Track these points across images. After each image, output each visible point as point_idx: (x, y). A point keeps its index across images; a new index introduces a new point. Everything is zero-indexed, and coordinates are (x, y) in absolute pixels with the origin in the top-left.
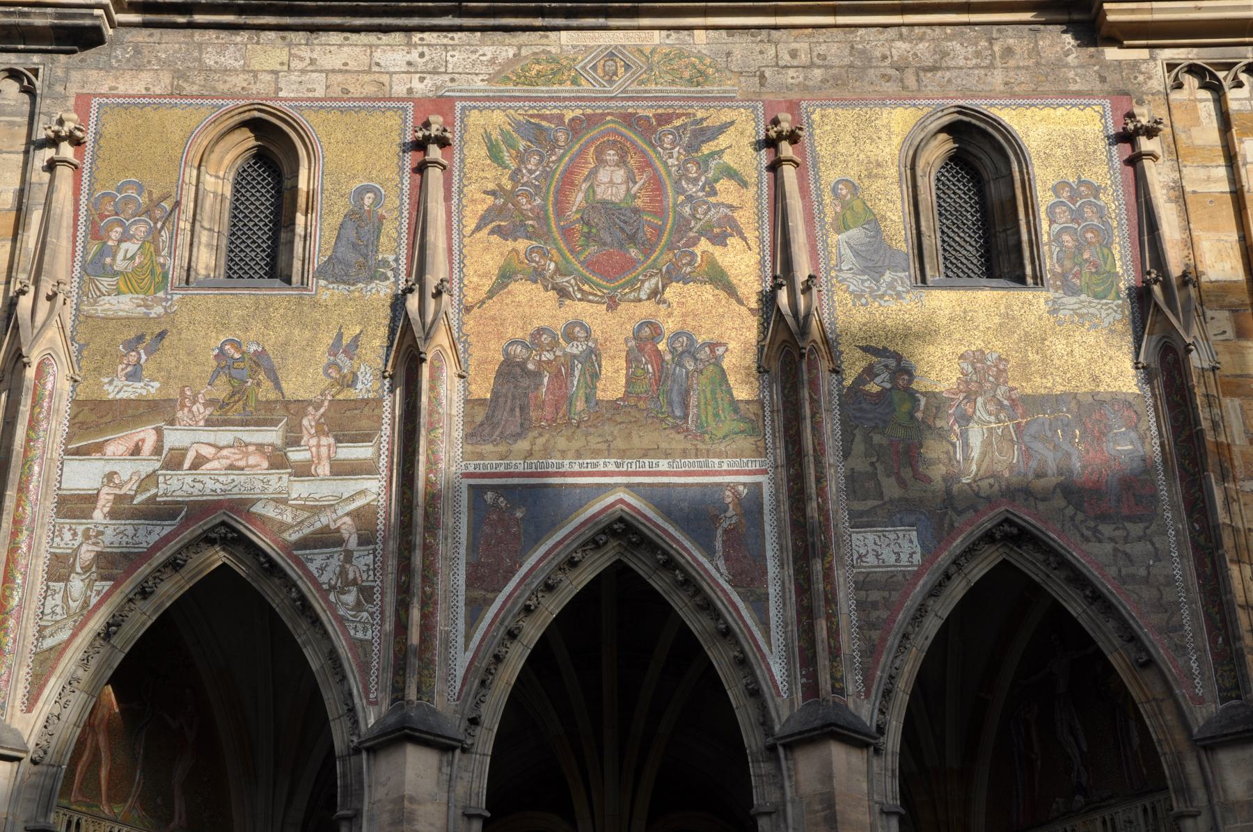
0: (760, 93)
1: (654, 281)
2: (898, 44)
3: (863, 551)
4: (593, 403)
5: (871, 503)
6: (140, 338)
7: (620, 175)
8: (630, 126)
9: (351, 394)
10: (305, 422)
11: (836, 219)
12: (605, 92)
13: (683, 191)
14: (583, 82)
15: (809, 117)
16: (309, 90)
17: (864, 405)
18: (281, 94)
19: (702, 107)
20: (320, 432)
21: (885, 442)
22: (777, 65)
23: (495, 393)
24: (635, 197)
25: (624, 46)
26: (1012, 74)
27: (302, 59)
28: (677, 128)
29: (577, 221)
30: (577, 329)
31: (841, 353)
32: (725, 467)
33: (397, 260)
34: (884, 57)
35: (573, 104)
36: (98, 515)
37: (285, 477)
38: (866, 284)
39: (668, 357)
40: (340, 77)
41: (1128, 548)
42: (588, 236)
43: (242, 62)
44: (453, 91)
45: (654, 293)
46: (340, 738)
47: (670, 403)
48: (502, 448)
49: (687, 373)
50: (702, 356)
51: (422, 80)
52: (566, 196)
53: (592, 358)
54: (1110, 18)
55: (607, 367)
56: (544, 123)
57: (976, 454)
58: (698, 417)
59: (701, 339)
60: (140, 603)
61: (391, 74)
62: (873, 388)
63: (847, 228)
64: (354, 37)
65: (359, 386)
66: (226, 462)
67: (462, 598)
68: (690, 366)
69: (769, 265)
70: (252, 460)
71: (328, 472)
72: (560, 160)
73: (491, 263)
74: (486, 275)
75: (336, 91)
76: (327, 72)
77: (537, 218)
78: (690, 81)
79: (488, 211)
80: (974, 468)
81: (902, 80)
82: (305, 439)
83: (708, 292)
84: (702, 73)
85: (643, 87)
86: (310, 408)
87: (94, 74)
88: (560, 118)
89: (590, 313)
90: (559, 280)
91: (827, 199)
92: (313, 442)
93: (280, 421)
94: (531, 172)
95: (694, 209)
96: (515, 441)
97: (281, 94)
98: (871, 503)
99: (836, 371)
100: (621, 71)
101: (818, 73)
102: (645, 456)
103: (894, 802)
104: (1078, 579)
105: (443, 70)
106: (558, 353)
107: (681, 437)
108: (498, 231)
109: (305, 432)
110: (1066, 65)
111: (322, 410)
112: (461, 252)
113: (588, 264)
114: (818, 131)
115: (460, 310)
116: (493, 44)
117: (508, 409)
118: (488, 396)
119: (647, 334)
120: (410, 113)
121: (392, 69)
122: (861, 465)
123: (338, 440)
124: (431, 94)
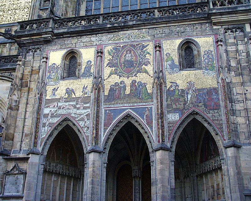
1: (135, 73)
3: (169, 118)
5: (170, 109)
6: (55, 89)
7: (130, 55)
9: (86, 95)
21: (174, 98)
26: (197, 32)
32: (146, 104)
34: (175, 31)
36: (49, 117)
39: (137, 86)
40: (85, 43)
41: (214, 115)
45: (135, 75)
46: (85, 152)
47: (137, 94)
48: (110, 103)
53: (125, 88)
54: (213, 21)
57: (189, 100)
60: (55, 131)
61: (93, 41)
62: (172, 89)
64: (88, 36)
65: (87, 94)
66: (67, 108)
67: (103, 129)
70: (71, 107)
71: (82, 108)
72: (120, 53)
80: (189, 102)
84: (144, 36)
85: (134, 40)
87: (49, 47)
89: (125, 79)
91: (165, 56)
96: (112, 102)
98: (170, 109)
103: (173, 159)
104: (206, 121)
108: (110, 66)
110: (207, 30)
122: (169, 103)
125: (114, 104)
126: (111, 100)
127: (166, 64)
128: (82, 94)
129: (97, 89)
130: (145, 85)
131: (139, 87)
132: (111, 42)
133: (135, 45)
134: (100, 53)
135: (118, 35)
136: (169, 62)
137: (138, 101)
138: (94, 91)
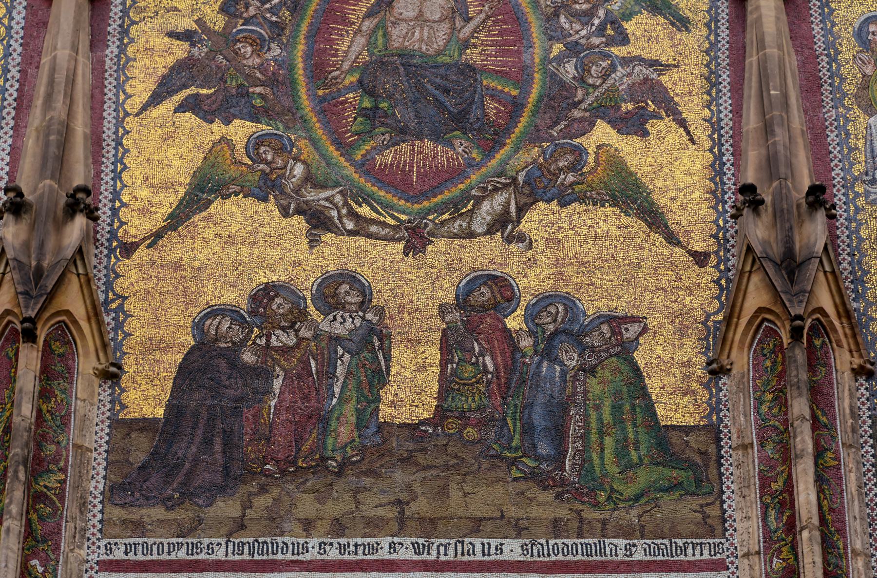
1: (500, 199)
23: (175, 410)
24: (466, 45)
29: (350, 89)
30: (345, 287)
32: (639, 556)
39: (526, 343)
42: (371, 115)
45: (501, 223)
47: (528, 429)
48: (183, 515)
49: (564, 373)
52: (331, 42)
53: (373, 342)
55: (401, 356)
58: (584, 455)
59: (592, 306)
73: (176, 163)
74: (167, 186)
77: (273, 81)
79: (180, 67)
83: (608, 220)
89: (376, 260)
90: (311, 195)
91: (848, 49)
106: (305, 333)
107: (550, 496)
108: (191, 105)
112: (119, 143)
113: (366, 167)
115: (112, 251)
117: (198, 440)
118: (160, 413)
125: (240, 526)
126: (203, 477)
129: (42, 334)
131: (548, 353)
137: (535, 512)
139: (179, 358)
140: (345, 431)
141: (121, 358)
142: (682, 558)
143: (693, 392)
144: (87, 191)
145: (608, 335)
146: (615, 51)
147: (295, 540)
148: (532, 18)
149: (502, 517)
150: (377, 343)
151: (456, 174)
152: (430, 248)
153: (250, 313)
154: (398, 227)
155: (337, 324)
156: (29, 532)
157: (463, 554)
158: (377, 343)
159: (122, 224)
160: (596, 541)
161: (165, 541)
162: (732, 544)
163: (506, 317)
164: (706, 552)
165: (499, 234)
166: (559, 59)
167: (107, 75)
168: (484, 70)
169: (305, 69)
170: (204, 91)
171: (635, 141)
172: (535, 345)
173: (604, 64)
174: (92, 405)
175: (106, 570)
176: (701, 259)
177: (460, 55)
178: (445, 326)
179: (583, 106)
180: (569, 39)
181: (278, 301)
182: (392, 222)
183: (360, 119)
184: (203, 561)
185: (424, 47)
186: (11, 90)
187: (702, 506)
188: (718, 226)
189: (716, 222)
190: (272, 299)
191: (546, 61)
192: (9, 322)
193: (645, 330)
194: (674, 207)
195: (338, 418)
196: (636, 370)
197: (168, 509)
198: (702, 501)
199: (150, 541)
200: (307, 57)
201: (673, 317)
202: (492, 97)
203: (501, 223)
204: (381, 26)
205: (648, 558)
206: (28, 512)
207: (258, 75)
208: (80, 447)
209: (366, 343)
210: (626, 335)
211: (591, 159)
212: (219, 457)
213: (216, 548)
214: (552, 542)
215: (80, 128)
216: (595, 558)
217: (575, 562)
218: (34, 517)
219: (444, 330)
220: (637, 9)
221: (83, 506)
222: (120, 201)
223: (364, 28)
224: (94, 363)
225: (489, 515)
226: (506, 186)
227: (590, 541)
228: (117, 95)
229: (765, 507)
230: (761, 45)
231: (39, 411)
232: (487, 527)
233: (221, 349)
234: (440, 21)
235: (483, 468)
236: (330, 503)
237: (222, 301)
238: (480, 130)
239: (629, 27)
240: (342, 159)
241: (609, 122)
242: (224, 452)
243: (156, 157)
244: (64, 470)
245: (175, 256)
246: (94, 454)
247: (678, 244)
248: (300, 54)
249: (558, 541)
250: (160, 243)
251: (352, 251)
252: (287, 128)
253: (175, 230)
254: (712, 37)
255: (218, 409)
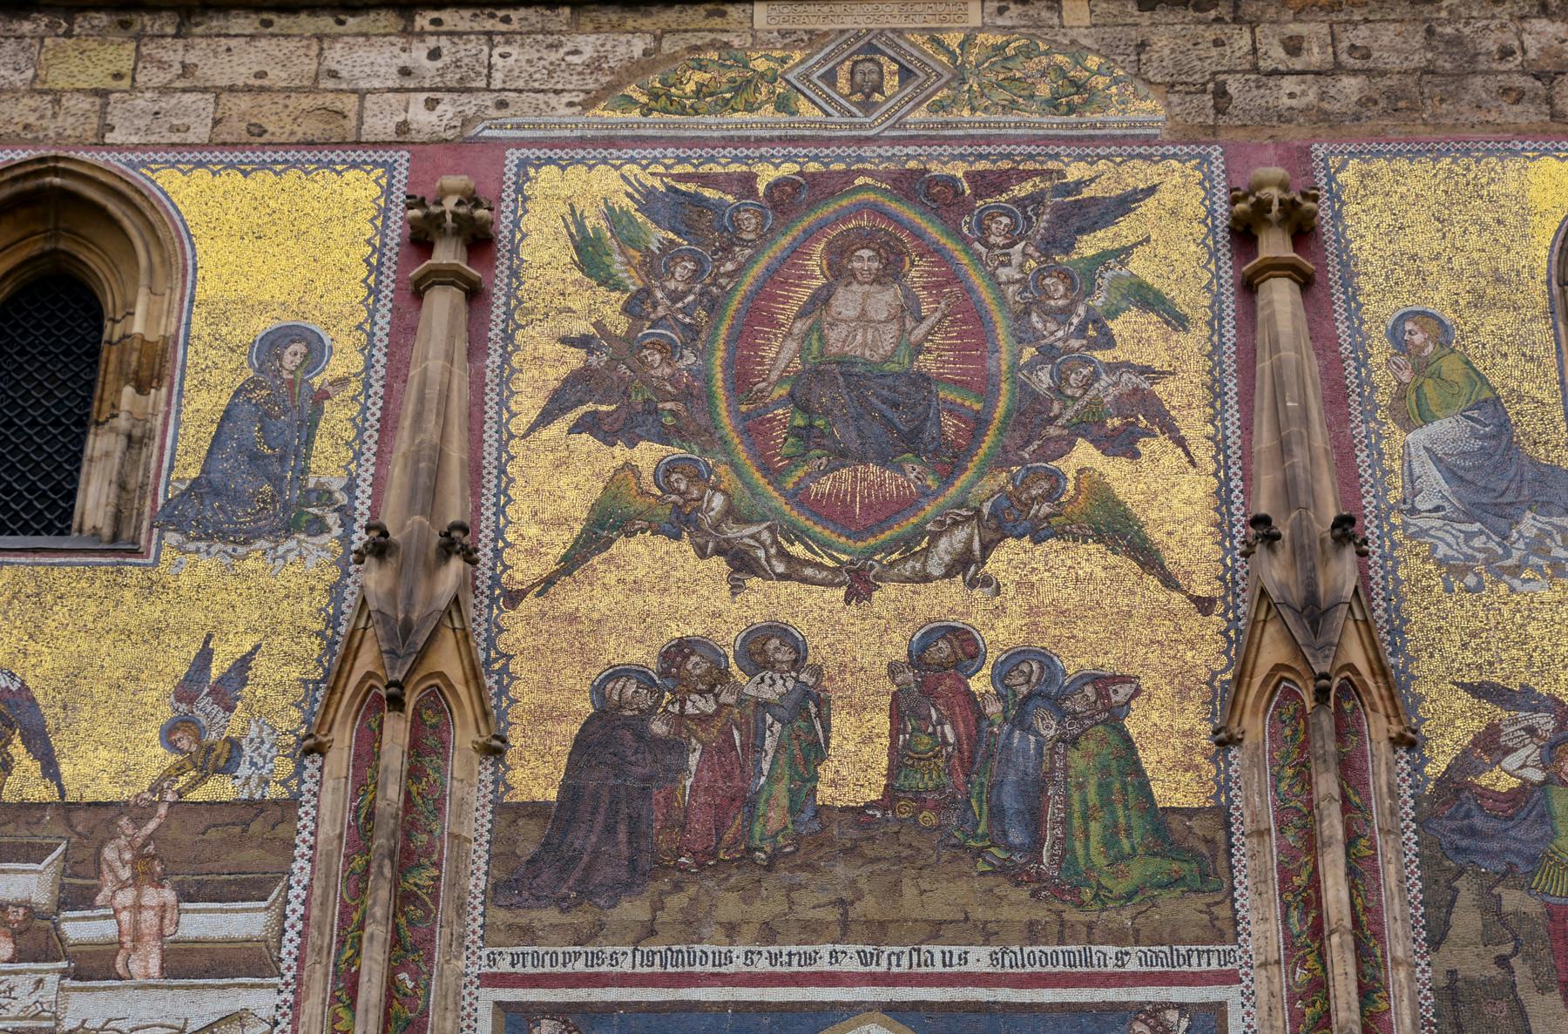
0: (1214, 128)
1: (960, 535)
2: (1540, 24)
4: (809, 813)
7: (884, 300)
8: (908, 196)
9: (220, 789)
10: (109, 853)
11: (1400, 396)
12: (853, 126)
13: (1036, 337)
14: (803, 105)
15: (1331, 179)
16: (174, 129)
17: (1478, 822)
18: (110, 138)
19: (1080, 158)
20: (145, 871)
21: (1533, 906)
22: (1255, 69)
23: (570, 792)
24: (918, 349)
25: (899, 32)
27: (162, 65)
28: (1016, 201)
29: (778, 403)
30: (774, 643)
31: (1420, 699)
32: (1132, 966)
33: (350, 488)
35: (780, 151)
37: (52, 980)
38: (1478, 542)
39: (993, 709)
40: (244, 102)
42: (805, 435)
43: (30, 73)
44: (502, 127)
45: (962, 564)
47: (997, 813)
48: (581, 918)
50: (1076, 704)
51: (431, 104)
52: (756, 347)
53: (809, 709)
56: (708, 193)
58: (1064, 841)
59: (1073, 663)
61: (362, 94)
62: (1500, 779)
63: (1426, 418)
65: (244, 770)
68: (1049, 728)
69: (1238, 499)
72: (741, 270)
74: (560, 522)
75: (235, 129)
76: (218, 92)
77: (686, 395)
78: (1053, 104)
79: (574, 379)
81: (1549, 101)
82: (106, 891)
83: (1092, 560)
85: (941, 117)
86: (124, 822)
88: (749, 180)
89: (812, 609)
90: (733, 532)
91: (1380, 350)
92: (126, 897)
93: (51, 849)
94: (675, 297)
95: (1061, 378)
97: (110, 138)
99: (1407, 742)
100: (891, 83)
101: (1351, 85)
102: (934, 937)
105: (483, 84)
106: (726, 698)
107: (1024, 894)
109: (108, 876)
111: (152, 826)
112: (502, 471)
113: (799, 498)
114: (1352, 208)
115: (494, 600)
116: (597, 30)
117: (598, 827)
118: (552, 795)
119: (940, 658)
120: (402, 174)
121: (363, 85)
122: (1475, 963)
123: (185, 896)
124: (450, 135)
125: (650, 931)
126: (604, 873)
127: (1411, 459)
128: (155, 758)
129: (411, 701)
130: (1108, 695)
131: (1020, 721)
132: (618, 116)
133: (951, 181)
134: (449, 244)
135: (712, 45)
136: (1446, 429)
137: (1006, 913)
138: (343, 740)
139: (576, 729)
140: (774, 816)
141: (506, 729)
142: (1185, 968)
143: (1197, 766)
144: (465, 530)
145: (1093, 699)
146: (1099, 355)
147: (716, 948)
148: (997, 317)
149: (967, 919)
150: (813, 710)
151: (907, 505)
152: (876, 594)
153: (660, 674)
154: (838, 569)
155: (765, 687)
156: (396, 940)
157: (919, 965)
158: (813, 710)
159: (506, 568)
160: (1081, 948)
161: (559, 950)
162: (1246, 952)
163: (969, 677)
164: (1214, 961)
165: (960, 577)
166: (1031, 366)
167: (487, 389)
168: (940, 379)
169: (724, 381)
170: (604, 408)
171: (1123, 464)
172: (1005, 711)
173: (1085, 372)
174: (471, 786)
175: (489, 986)
176: (1204, 605)
177: (911, 362)
178: (895, 688)
179: (1060, 422)
180: (1043, 342)
181: (694, 659)
182: (831, 564)
183: (791, 440)
184: (606, 975)
185: (867, 353)
186: (374, 409)
187: (1209, 905)
188: (1225, 565)
189: (1222, 561)
190: (687, 657)
191: (1015, 367)
192: (372, 687)
193: (1138, 692)
194: (1172, 543)
195: (767, 801)
196: (1127, 739)
197: (562, 911)
198: (1209, 900)
199: (542, 950)
200: (727, 366)
201: (1171, 676)
202: (950, 412)
203: (962, 564)
204: (816, 328)
205: (1145, 969)
206: (395, 915)
207: (669, 388)
208: (457, 837)
209: (800, 710)
210: (1114, 698)
211: (1070, 486)
212: (624, 849)
213: (621, 958)
214: (1027, 950)
215: (456, 453)
216: (1079, 969)
217: (1056, 974)
218: (403, 921)
219: (894, 694)
220: (1124, 304)
221: (461, 908)
222: (504, 540)
223: (796, 331)
224: (474, 736)
225: (951, 917)
226: (968, 519)
227: (1074, 948)
228: (499, 414)
229: (1286, 907)
230: (1275, 347)
231: (408, 794)
232: (948, 931)
233: (626, 718)
234: (887, 321)
235: (945, 858)
236: (758, 903)
237: (627, 660)
238: (936, 452)
239: (1115, 326)
240: (770, 488)
241: (1092, 442)
242: (630, 842)
243: (546, 487)
244: (437, 865)
245: (569, 606)
246: (474, 846)
247: (1177, 587)
248: (719, 362)
249: (1034, 948)
250: (552, 590)
251: (783, 598)
252: (704, 451)
253: (570, 575)
254: (1215, 338)
255: (623, 792)
